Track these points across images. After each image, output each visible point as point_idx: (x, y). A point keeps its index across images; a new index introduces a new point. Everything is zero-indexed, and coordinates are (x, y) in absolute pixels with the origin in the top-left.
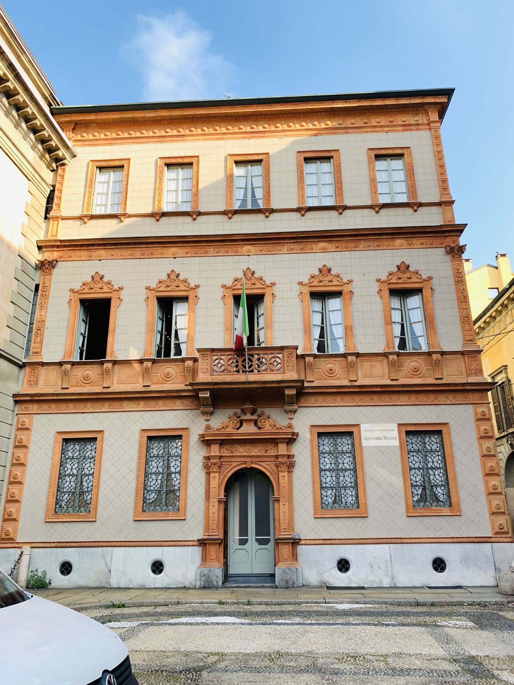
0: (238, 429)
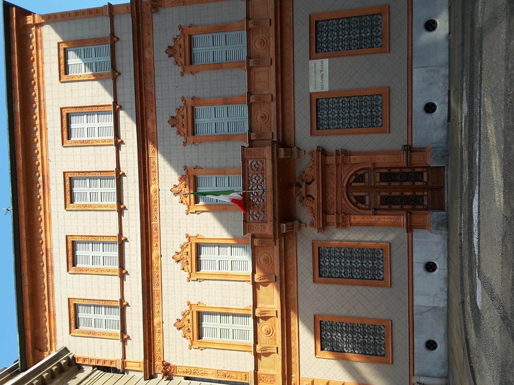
0: (313, 199)
